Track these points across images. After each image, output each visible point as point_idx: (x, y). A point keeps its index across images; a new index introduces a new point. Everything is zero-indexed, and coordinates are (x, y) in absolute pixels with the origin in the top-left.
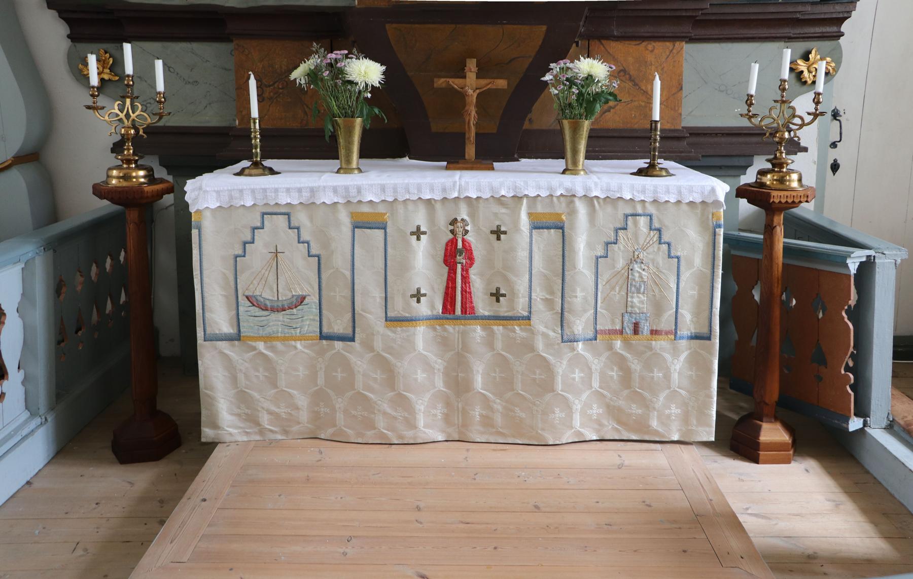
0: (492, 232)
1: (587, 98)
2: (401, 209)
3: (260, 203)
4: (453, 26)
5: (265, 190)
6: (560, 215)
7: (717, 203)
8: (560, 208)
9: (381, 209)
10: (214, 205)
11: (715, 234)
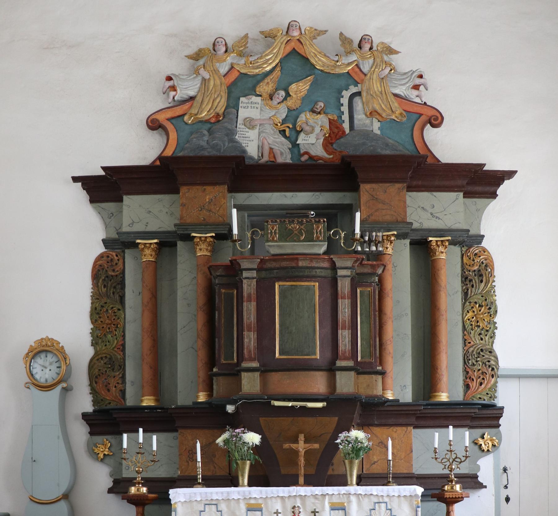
0: (312, 512)
1: (357, 449)
2: (269, 502)
3: (204, 499)
4: (292, 418)
5: (206, 493)
6: (344, 503)
7: (416, 496)
8: (344, 500)
9: (260, 501)
10: (183, 500)
11: (417, 511)
